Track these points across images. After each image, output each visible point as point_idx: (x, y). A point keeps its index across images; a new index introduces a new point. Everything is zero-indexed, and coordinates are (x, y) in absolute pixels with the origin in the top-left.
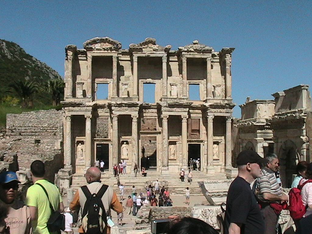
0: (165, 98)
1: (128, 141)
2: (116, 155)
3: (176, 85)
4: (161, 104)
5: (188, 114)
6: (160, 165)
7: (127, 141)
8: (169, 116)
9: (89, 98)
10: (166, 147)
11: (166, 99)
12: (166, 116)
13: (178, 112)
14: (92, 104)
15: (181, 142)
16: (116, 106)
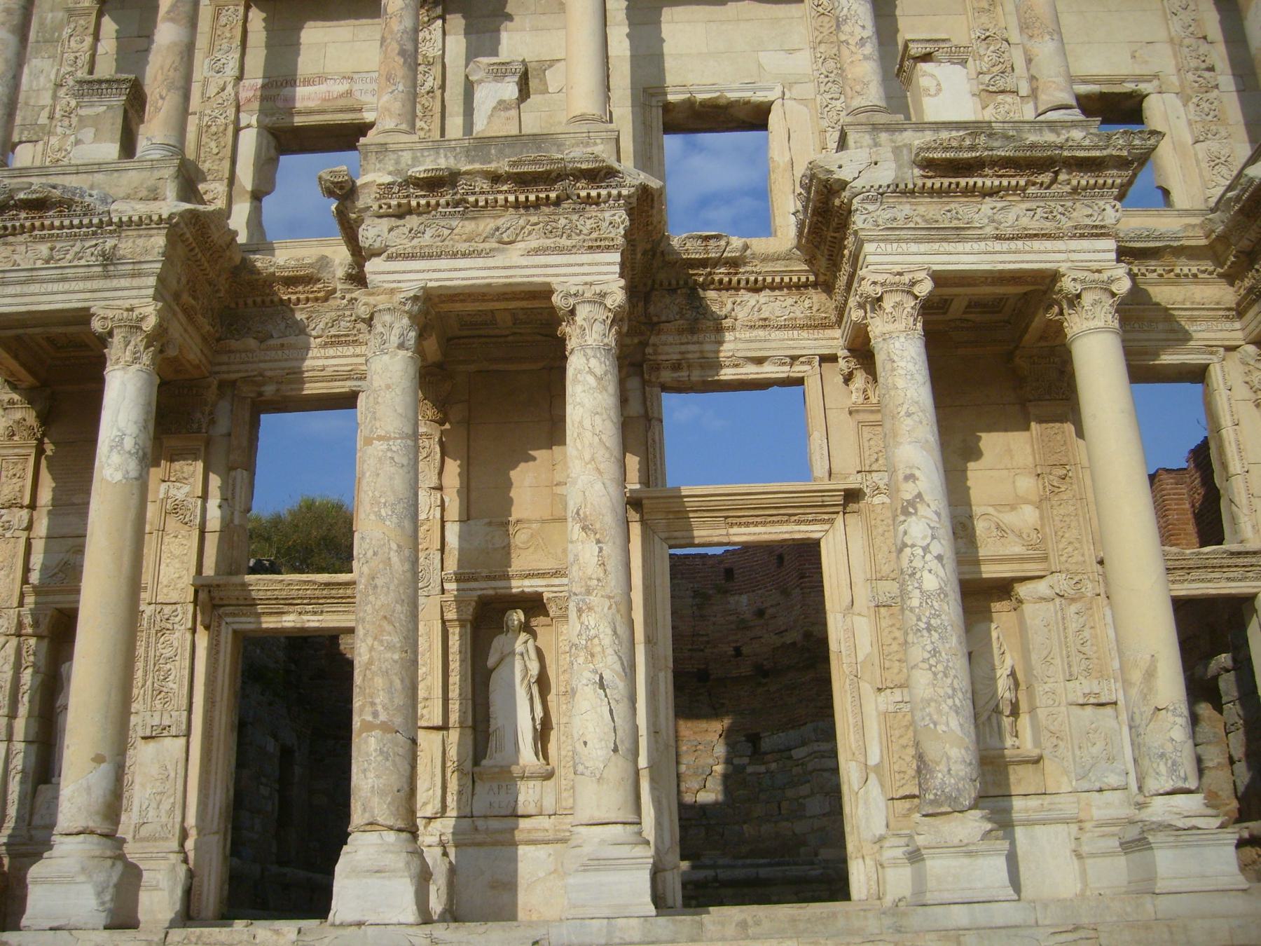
0: (875, 128)
1: (546, 596)
2: (390, 690)
3: (959, 57)
4: (845, 175)
5: (1118, 260)
6: (880, 830)
7: (540, 595)
8: (940, 279)
9: (153, 165)
10: (942, 592)
11: (884, 136)
12: (906, 278)
13: (1019, 244)
14: (170, 205)
15: (1061, 582)
16: (402, 213)
